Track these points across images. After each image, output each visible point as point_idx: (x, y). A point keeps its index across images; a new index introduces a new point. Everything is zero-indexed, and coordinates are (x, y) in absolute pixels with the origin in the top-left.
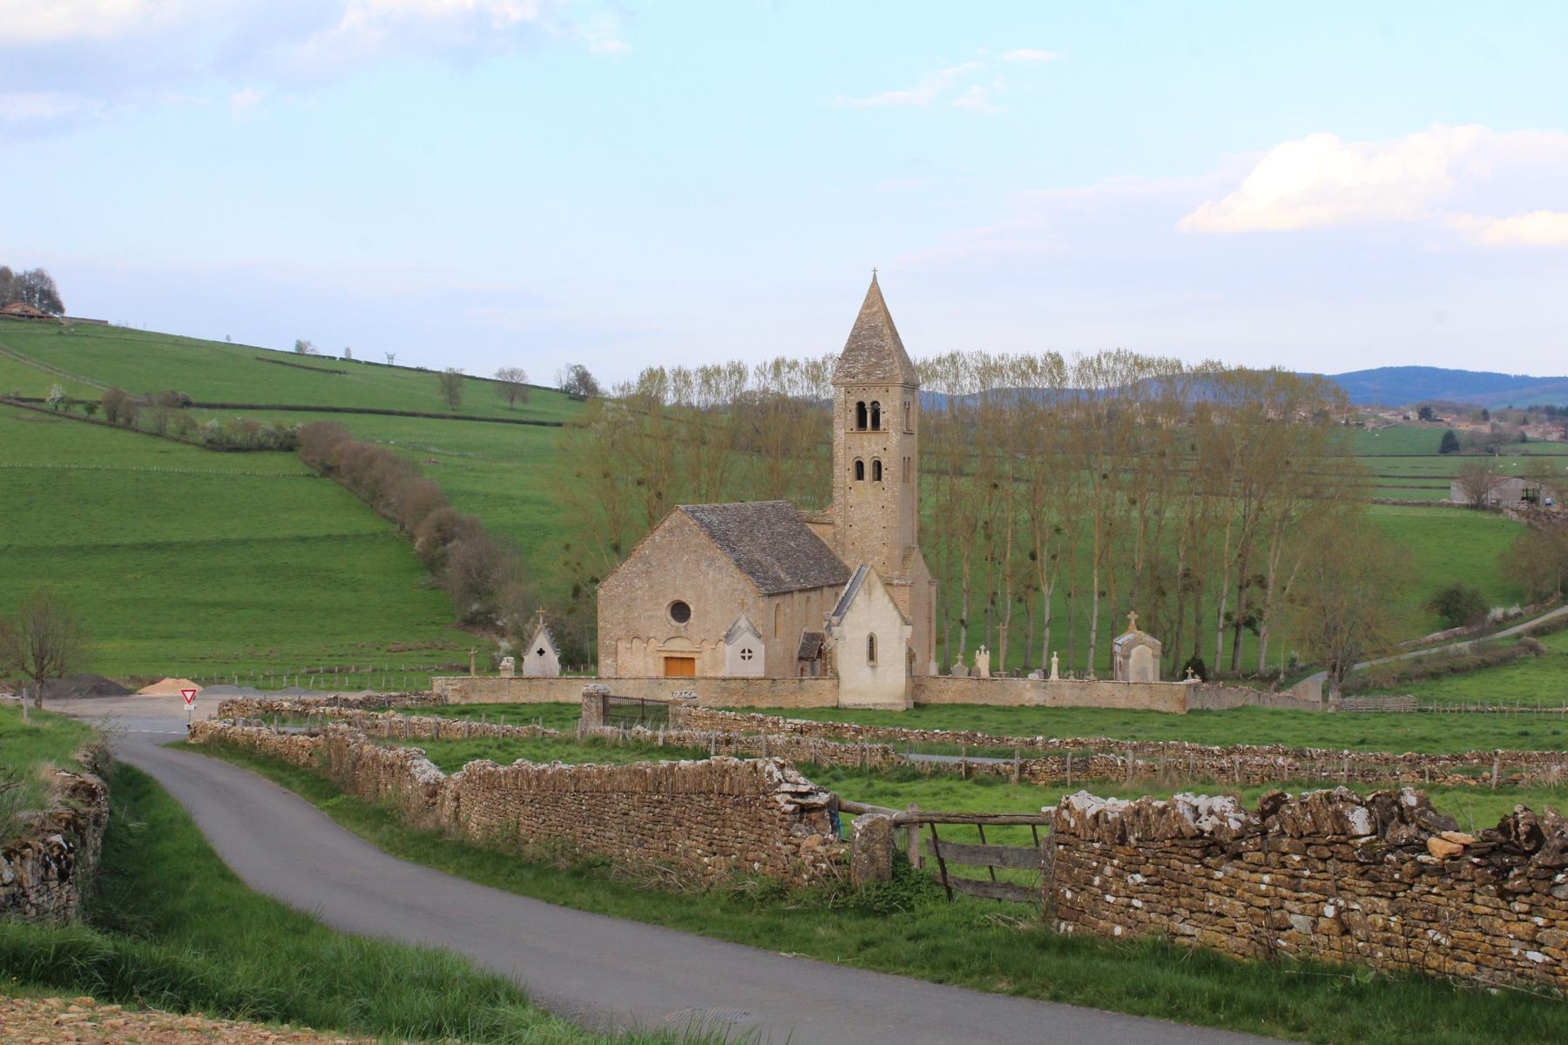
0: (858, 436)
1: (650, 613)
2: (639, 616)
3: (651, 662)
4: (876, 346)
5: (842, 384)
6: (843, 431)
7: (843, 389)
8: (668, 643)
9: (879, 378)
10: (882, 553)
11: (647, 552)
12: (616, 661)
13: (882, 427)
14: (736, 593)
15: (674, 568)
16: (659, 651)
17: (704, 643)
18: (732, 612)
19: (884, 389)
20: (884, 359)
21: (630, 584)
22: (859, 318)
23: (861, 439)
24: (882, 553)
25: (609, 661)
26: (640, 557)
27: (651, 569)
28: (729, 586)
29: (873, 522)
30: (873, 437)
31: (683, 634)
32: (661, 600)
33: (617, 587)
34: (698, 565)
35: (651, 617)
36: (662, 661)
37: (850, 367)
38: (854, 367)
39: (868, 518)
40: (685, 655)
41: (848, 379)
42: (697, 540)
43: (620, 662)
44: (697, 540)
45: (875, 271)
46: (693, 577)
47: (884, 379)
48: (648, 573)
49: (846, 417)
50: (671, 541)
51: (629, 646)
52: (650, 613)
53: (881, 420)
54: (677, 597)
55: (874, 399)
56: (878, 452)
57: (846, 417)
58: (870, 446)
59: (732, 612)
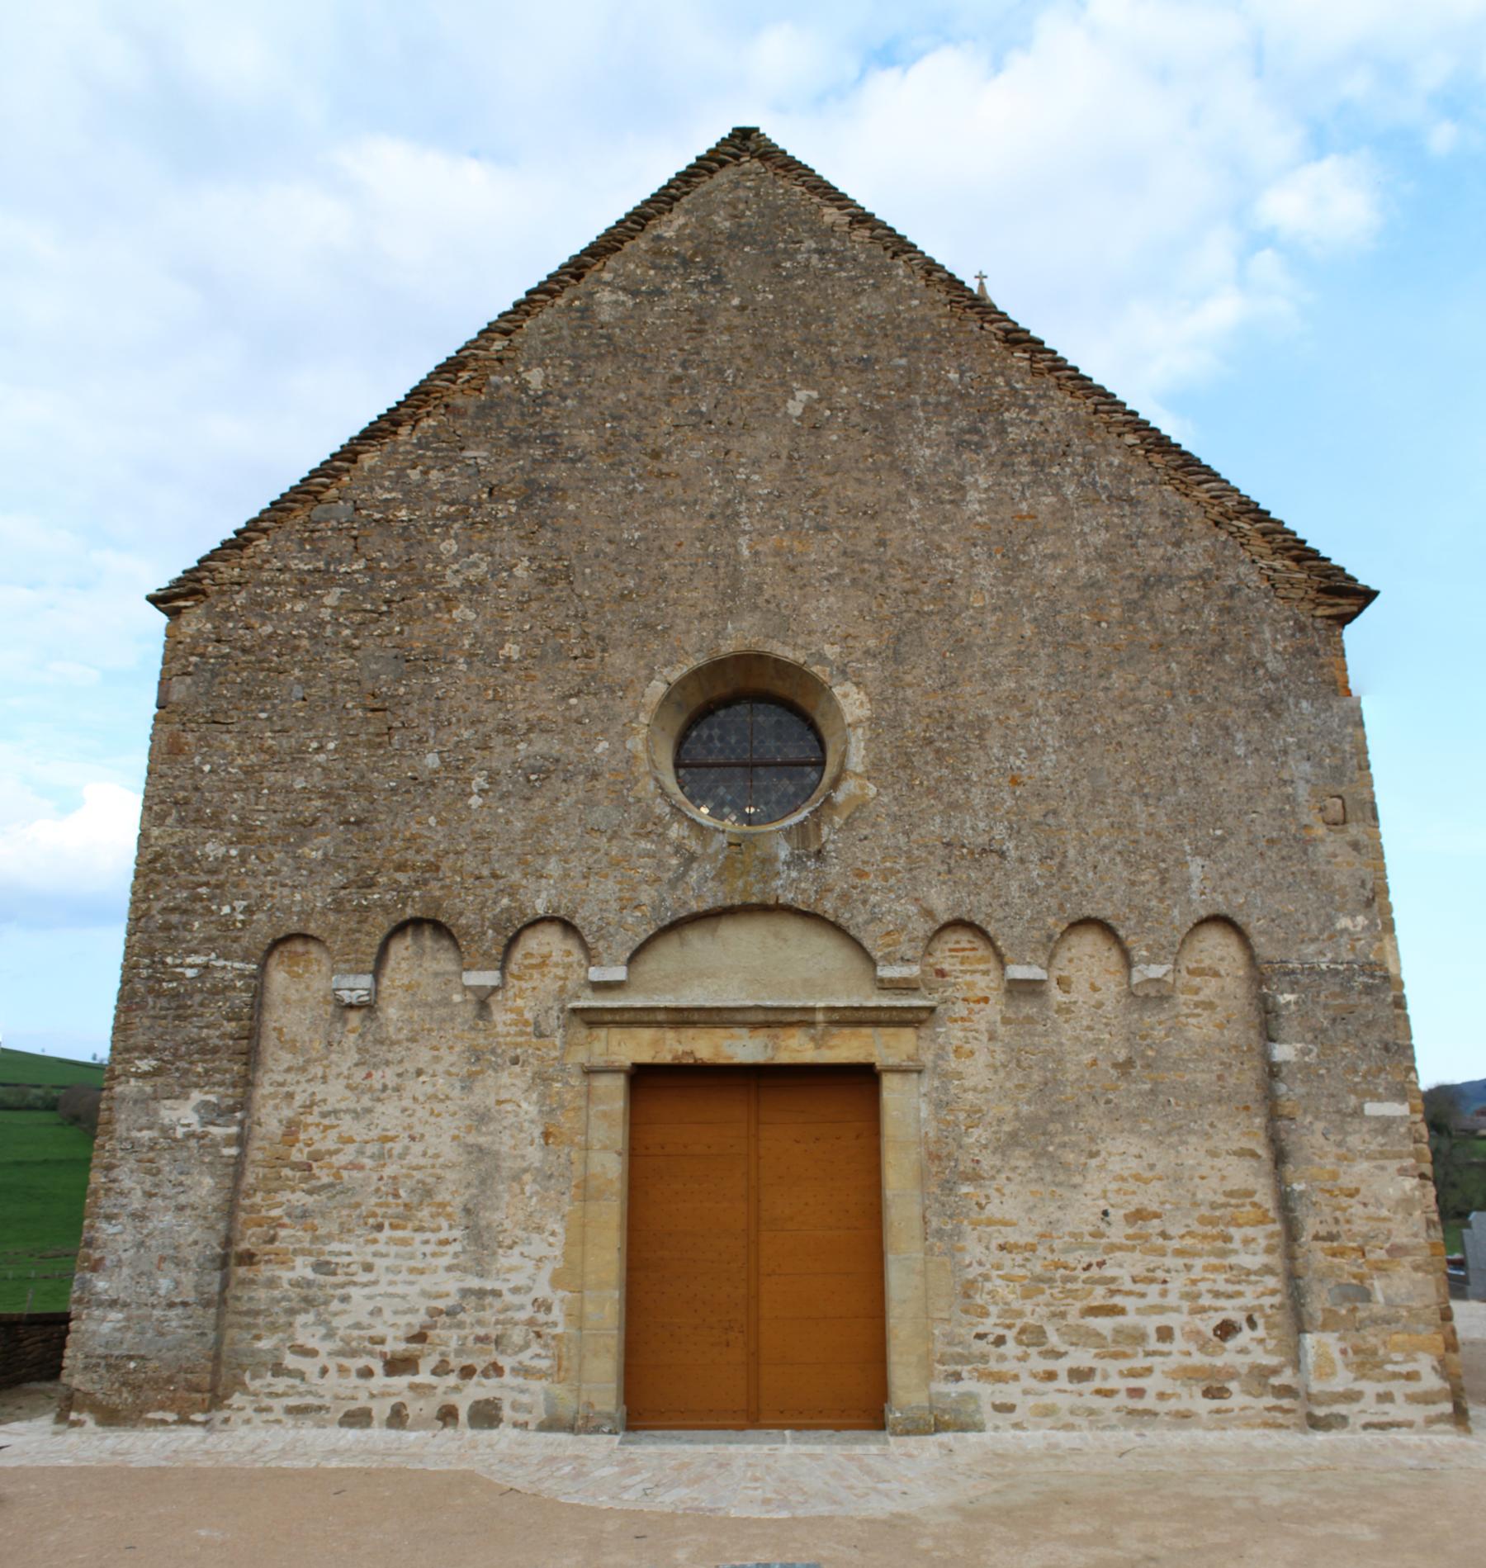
1: (541, 744)
2: (456, 767)
3: (529, 1109)
8: (668, 957)
11: (535, 378)
12: (243, 1105)
14: (1168, 600)
15: (722, 462)
16: (592, 1019)
17: (945, 955)
18: (1154, 722)
21: (409, 567)
25: (183, 1114)
26: (483, 410)
27: (555, 473)
28: (1106, 556)
31: (787, 886)
32: (620, 660)
33: (305, 587)
34: (887, 442)
35: (543, 772)
36: (614, 1089)
40: (797, 1049)
42: (871, 304)
43: (270, 1118)
44: (871, 304)
46: (851, 511)
48: (530, 492)
50: (700, 327)
51: (357, 986)
52: (541, 744)
54: (739, 636)
59: (1154, 722)
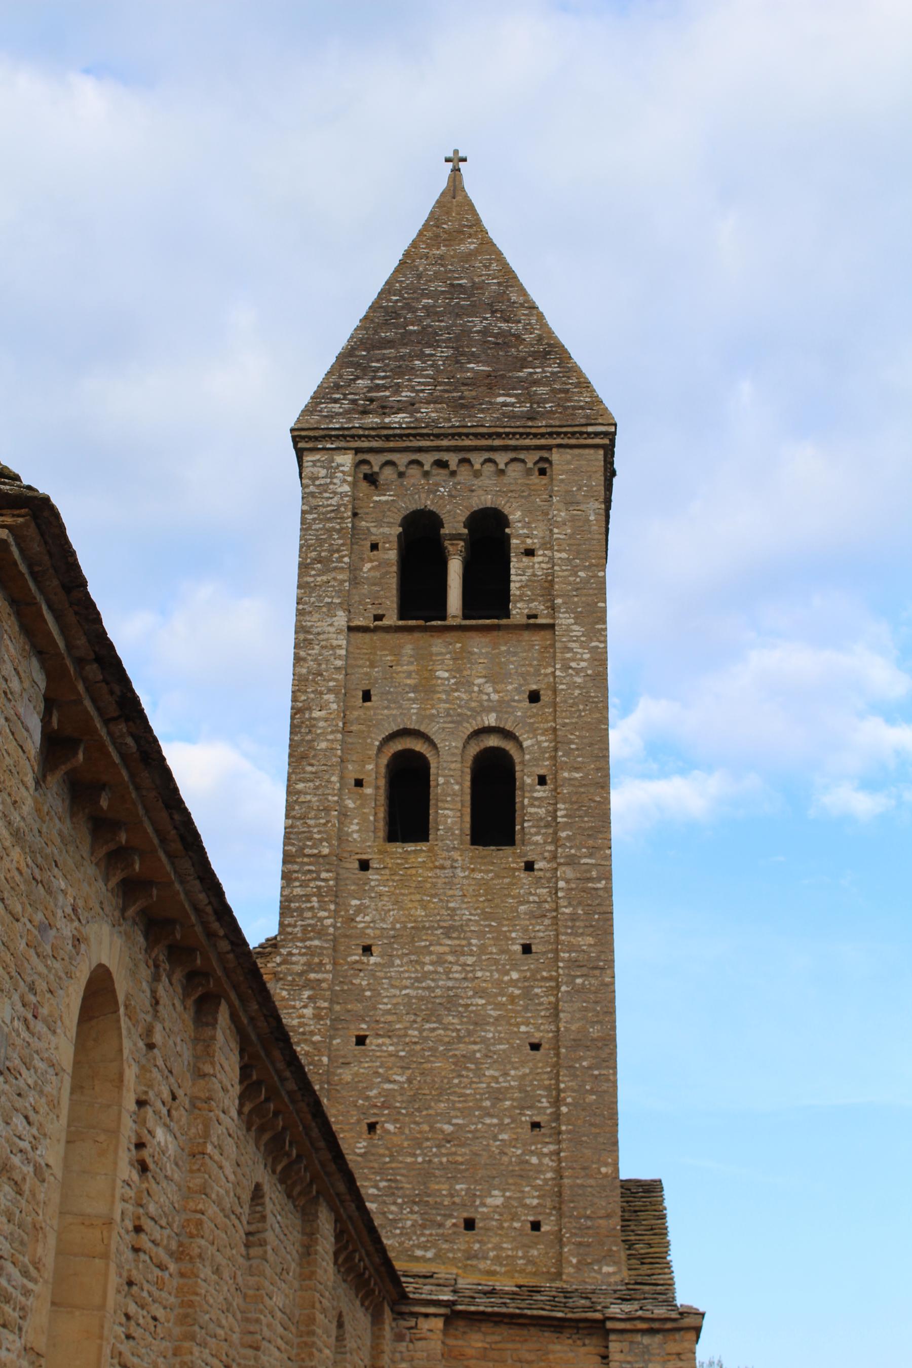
0: (408, 645)
4: (485, 332)
5: (344, 435)
6: (341, 620)
7: (346, 460)
9: (513, 416)
10: (524, 1173)
13: (518, 610)
19: (531, 458)
20: (523, 363)
22: (404, 265)
23: (423, 657)
24: (524, 1173)
29: (479, 1022)
30: (479, 645)
37: (378, 388)
38: (397, 389)
39: (451, 1002)
41: (373, 420)
45: (456, 160)
47: (531, 416)
49: (354, 570)
53: (514, 587)
55: (487, 500)
56: (500, 707)
57: (354, 570)
58: (464, 683)
